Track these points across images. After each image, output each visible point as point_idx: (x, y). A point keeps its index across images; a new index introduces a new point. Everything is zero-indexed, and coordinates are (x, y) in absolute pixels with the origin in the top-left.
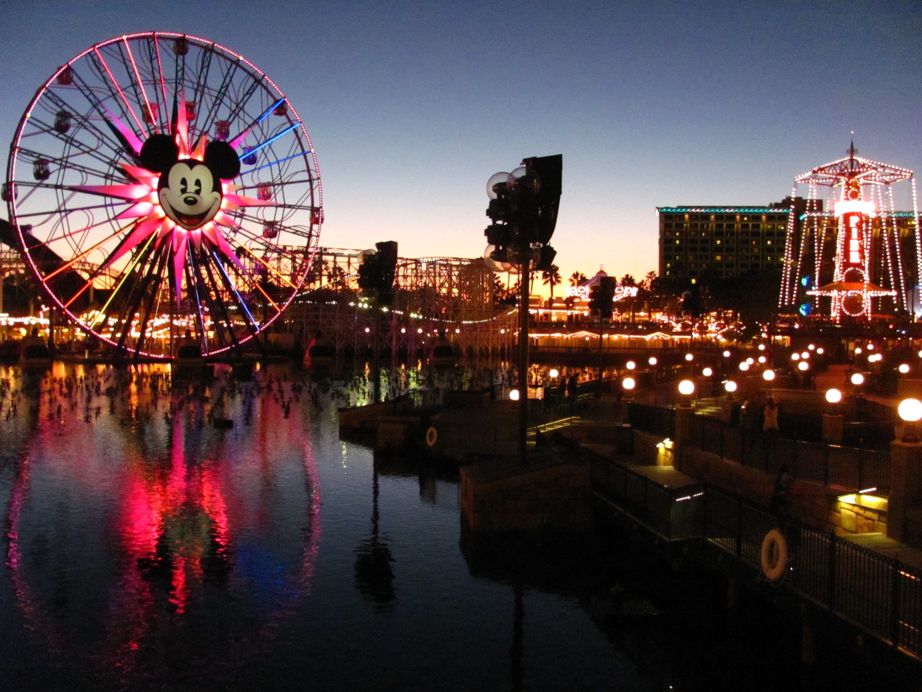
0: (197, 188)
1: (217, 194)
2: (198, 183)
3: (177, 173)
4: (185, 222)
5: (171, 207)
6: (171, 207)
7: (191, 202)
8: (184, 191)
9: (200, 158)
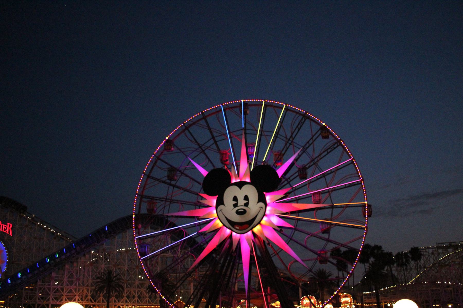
0: (246, 202)
1: (262, 204)
2: (246, 198)
7: (241, 213)
8: (235, 206)
9: (248, 180)
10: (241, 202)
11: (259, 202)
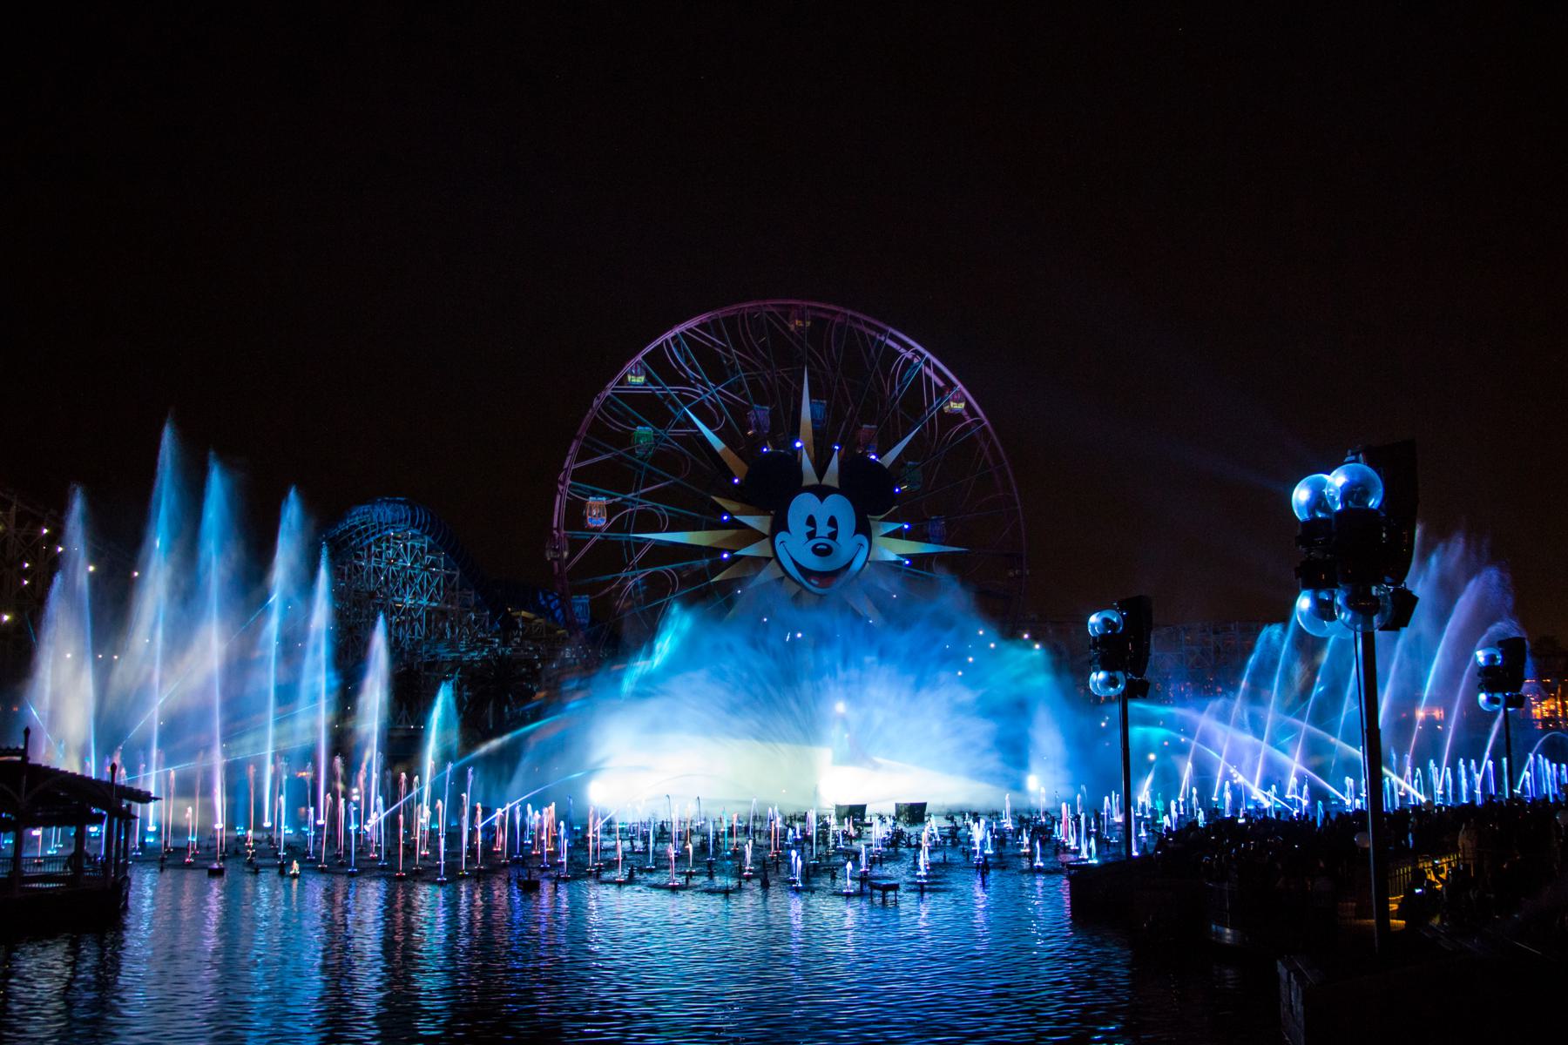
0: (834, 530)
1: (862, 538)
2: (832, 522)
3: (803, 506)
4: (813, 581)
5: (792, 558)
6: (792, 558)
8: (811, 535)
9: (835, 484)
10: (823, 529)
11: (856, 532)
